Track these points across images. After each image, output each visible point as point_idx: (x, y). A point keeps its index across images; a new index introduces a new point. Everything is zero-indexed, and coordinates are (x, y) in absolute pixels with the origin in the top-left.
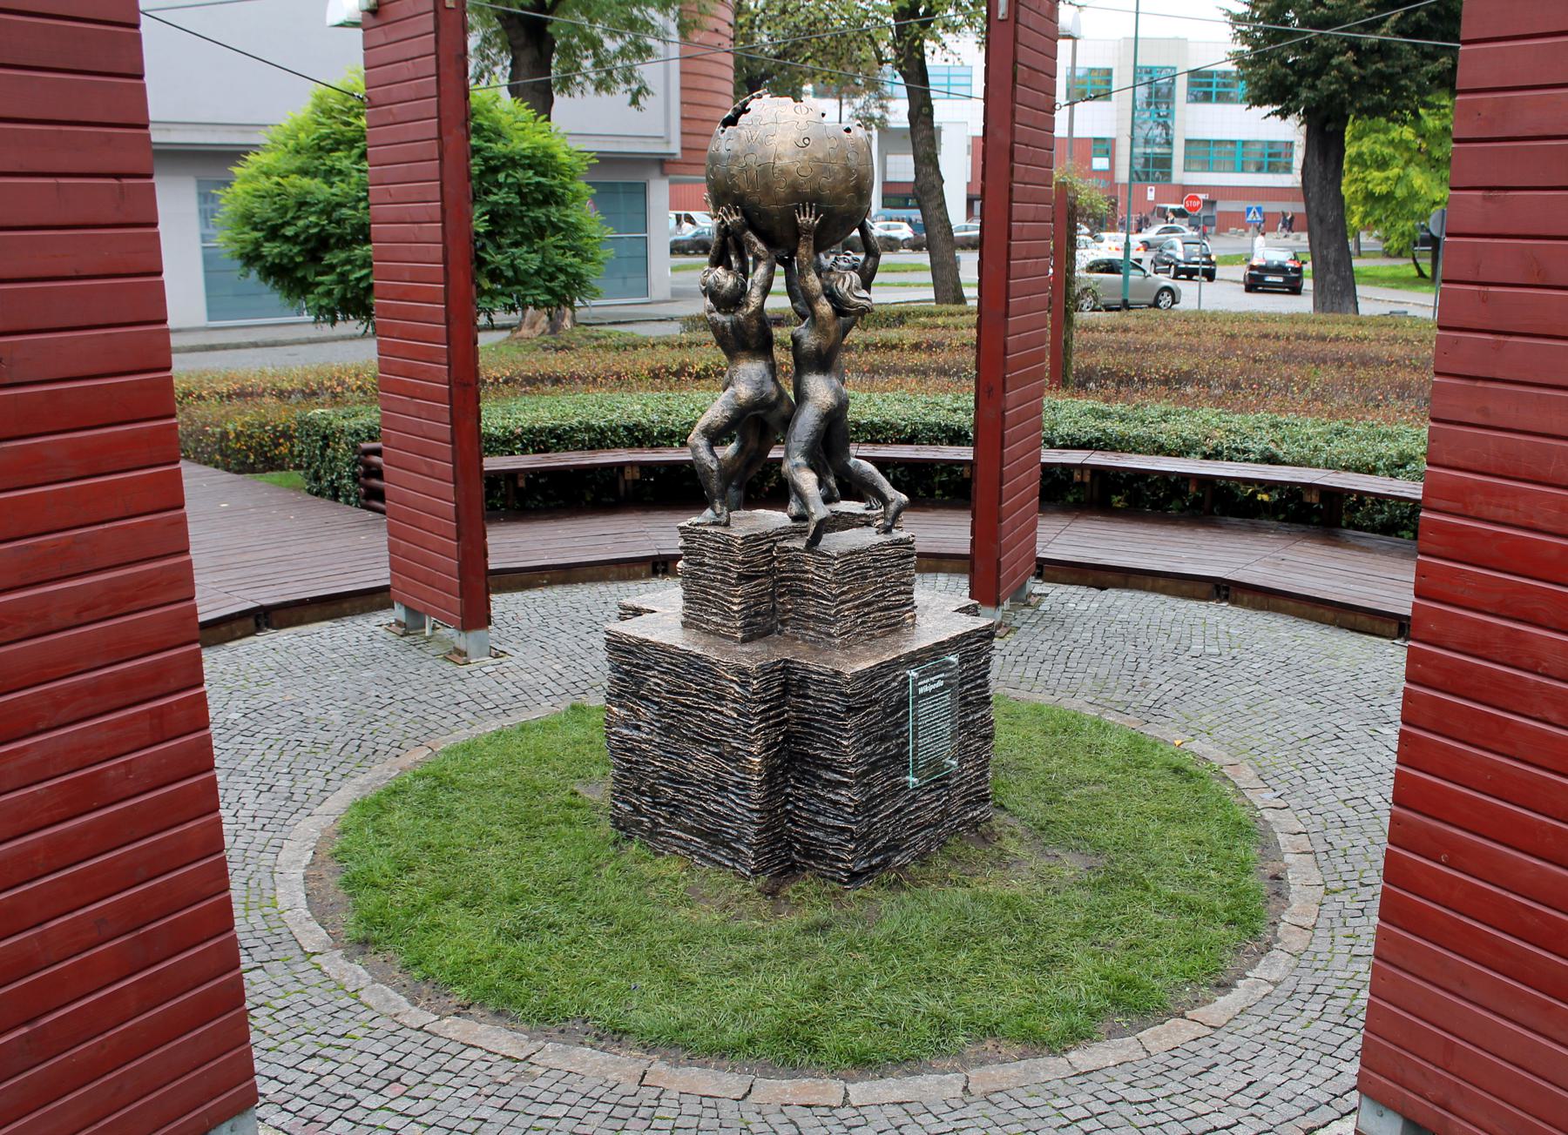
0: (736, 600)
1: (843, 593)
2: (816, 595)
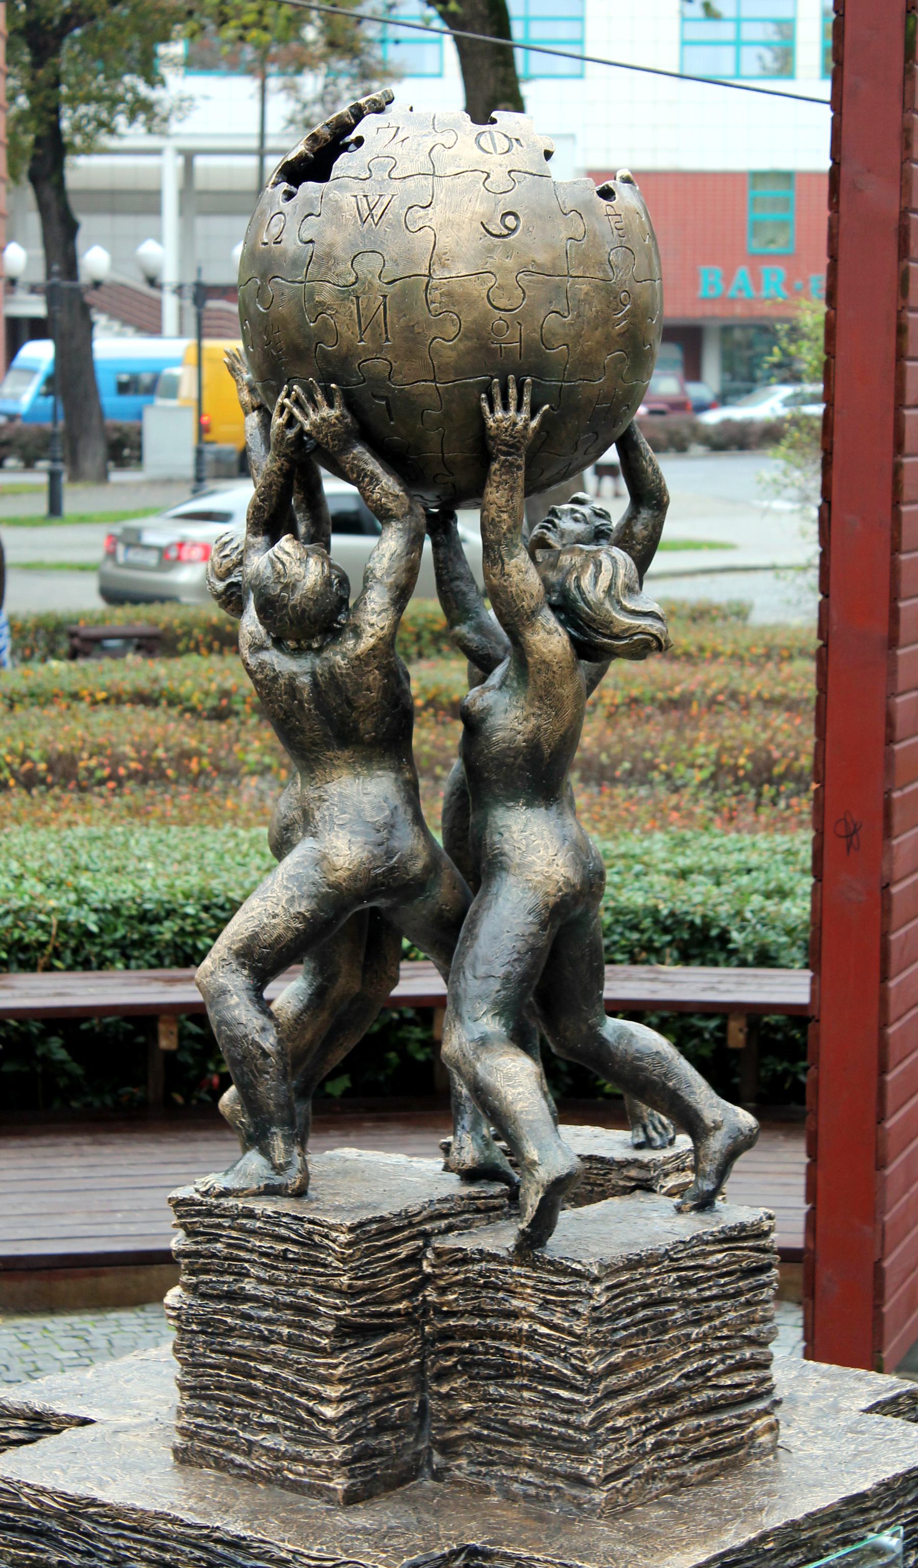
0: (333, 1392)
1: (613, 1369)
2: (541, 1375)
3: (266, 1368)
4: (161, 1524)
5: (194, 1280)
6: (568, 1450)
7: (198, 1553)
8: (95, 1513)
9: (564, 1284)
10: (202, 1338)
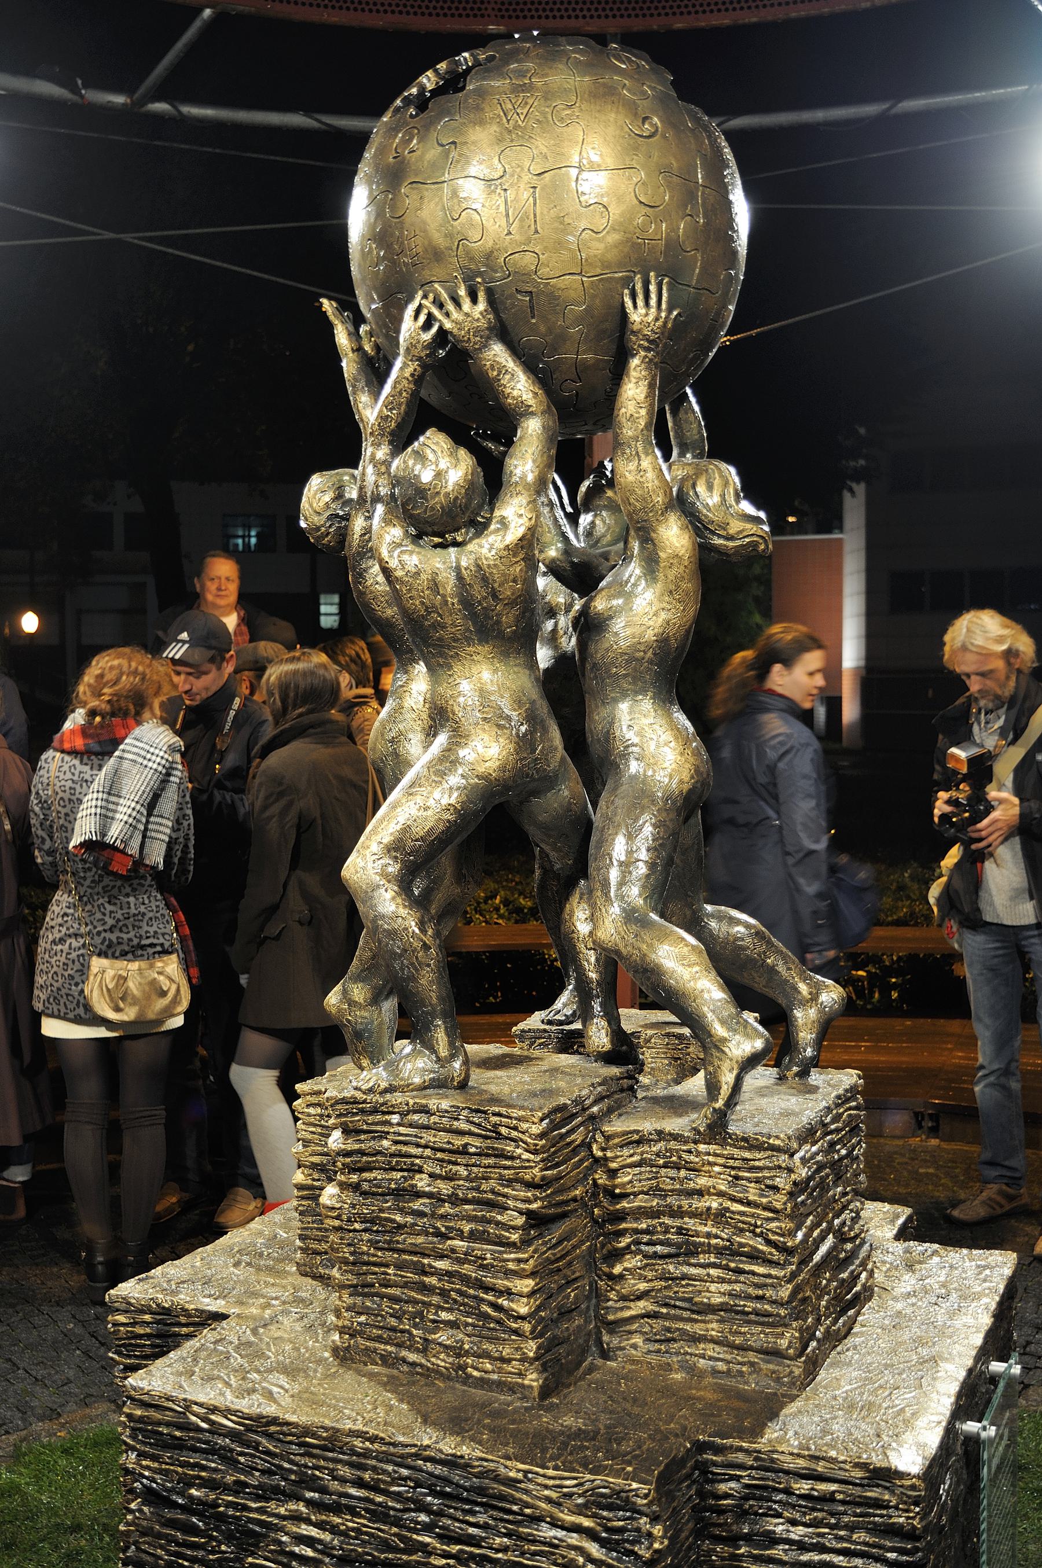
3: (441, 1265)
4: (358, 1443)
5: (354, 1178)
6: (762, 1324)
7: (405, 1472)
8: (278, 1432)
9: (759, 1160)
10: (366, 1236)
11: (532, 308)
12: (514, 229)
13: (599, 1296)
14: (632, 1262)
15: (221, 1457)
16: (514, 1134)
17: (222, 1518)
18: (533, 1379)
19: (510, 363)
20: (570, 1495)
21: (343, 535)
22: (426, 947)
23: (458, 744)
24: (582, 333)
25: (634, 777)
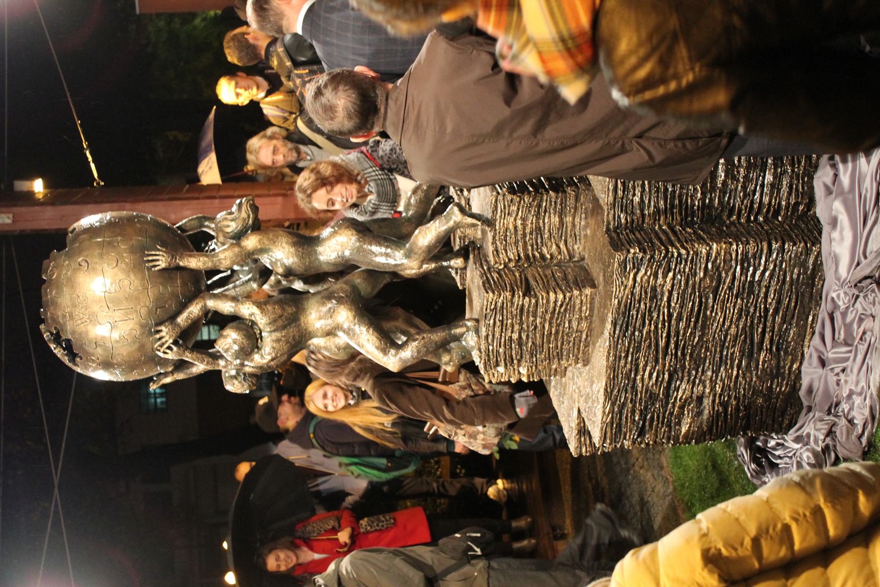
4: (611, 359)
5: (515, 362)
6: (566, 201)
7: (620, 341)
10: (538, 356)
11: (162, 307)
12: (131, 317)
13: (559, 264)
14: (545, 250)
15: (623, 408)
16: (493, 303)
17: (646, 408)
18: (588, 291)
19: (185, 315)
20: (622, 282)
21: (252, 375)
22: (423, 338)
23: (341, 328)
24: (170, 286)
25: (351, 254)
